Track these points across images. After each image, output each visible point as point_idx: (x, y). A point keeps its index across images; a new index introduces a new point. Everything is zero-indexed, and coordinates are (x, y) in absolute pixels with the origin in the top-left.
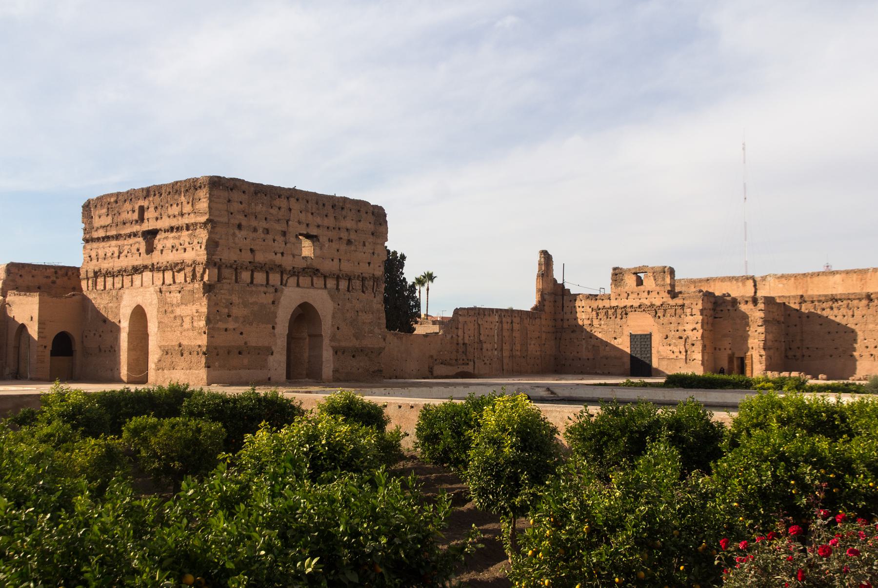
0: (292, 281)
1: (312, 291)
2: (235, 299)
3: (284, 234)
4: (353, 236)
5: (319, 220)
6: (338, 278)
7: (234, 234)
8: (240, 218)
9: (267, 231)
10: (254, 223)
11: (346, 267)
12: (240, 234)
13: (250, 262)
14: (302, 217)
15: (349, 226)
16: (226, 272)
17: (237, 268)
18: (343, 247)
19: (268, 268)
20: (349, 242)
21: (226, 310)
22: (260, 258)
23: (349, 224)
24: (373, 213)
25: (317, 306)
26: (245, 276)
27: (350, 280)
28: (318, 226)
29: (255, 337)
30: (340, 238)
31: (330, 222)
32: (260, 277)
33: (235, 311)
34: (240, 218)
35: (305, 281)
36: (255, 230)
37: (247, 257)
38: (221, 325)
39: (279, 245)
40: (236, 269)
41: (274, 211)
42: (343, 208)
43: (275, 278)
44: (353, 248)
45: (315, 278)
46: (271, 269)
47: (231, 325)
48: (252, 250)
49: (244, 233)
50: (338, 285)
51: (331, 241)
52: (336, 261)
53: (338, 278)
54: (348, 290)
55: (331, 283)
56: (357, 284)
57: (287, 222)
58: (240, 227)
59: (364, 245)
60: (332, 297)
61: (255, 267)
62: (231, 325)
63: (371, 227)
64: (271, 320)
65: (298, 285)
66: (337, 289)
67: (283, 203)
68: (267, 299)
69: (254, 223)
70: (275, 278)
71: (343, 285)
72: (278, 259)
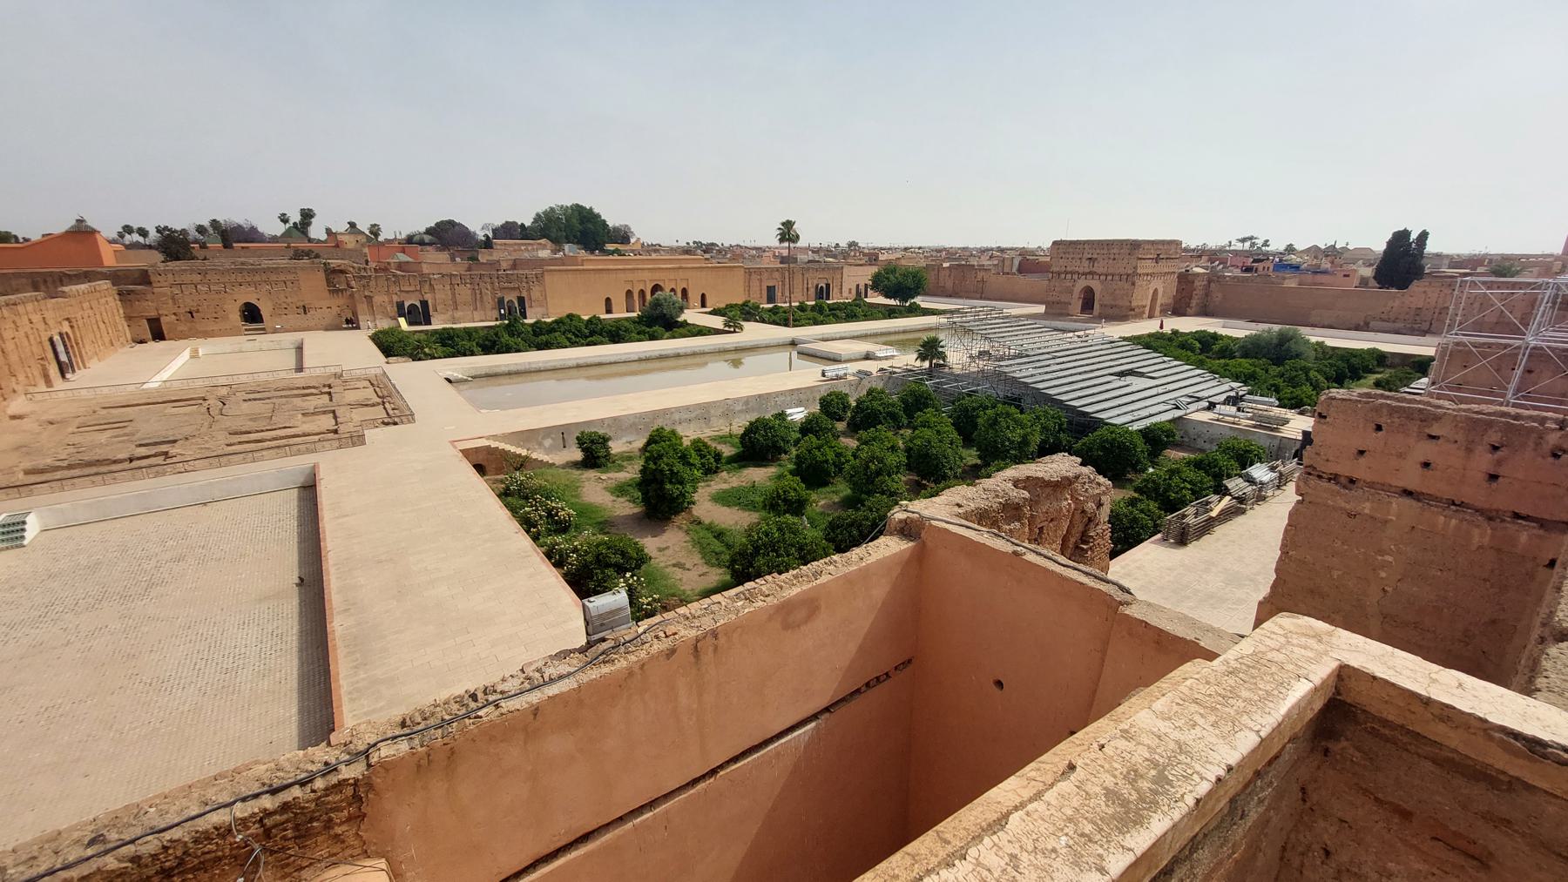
2: (1057, 284)
4: (1117, 256)
5: (1098, 251)
6: (1106, 276)
10: (1067, 256)
17: (1059, 274)
18: (1111, 261)
19: (1072, 273)
20: (1114, 259)
22: (1069, 269)
26: (1063, 276)
29: (1063, 298)
32: (1069, 276)
35: (1089, 277)
43: (1075, 277)
53: (1106, 276)
56: (1117, 278)
60: (1102, 282)
61: (1066, 273)
63: (1129, 251)
64: (1071, 292)
69: (1067, 256)
70: (1075, 277)
71: (1110, 278)
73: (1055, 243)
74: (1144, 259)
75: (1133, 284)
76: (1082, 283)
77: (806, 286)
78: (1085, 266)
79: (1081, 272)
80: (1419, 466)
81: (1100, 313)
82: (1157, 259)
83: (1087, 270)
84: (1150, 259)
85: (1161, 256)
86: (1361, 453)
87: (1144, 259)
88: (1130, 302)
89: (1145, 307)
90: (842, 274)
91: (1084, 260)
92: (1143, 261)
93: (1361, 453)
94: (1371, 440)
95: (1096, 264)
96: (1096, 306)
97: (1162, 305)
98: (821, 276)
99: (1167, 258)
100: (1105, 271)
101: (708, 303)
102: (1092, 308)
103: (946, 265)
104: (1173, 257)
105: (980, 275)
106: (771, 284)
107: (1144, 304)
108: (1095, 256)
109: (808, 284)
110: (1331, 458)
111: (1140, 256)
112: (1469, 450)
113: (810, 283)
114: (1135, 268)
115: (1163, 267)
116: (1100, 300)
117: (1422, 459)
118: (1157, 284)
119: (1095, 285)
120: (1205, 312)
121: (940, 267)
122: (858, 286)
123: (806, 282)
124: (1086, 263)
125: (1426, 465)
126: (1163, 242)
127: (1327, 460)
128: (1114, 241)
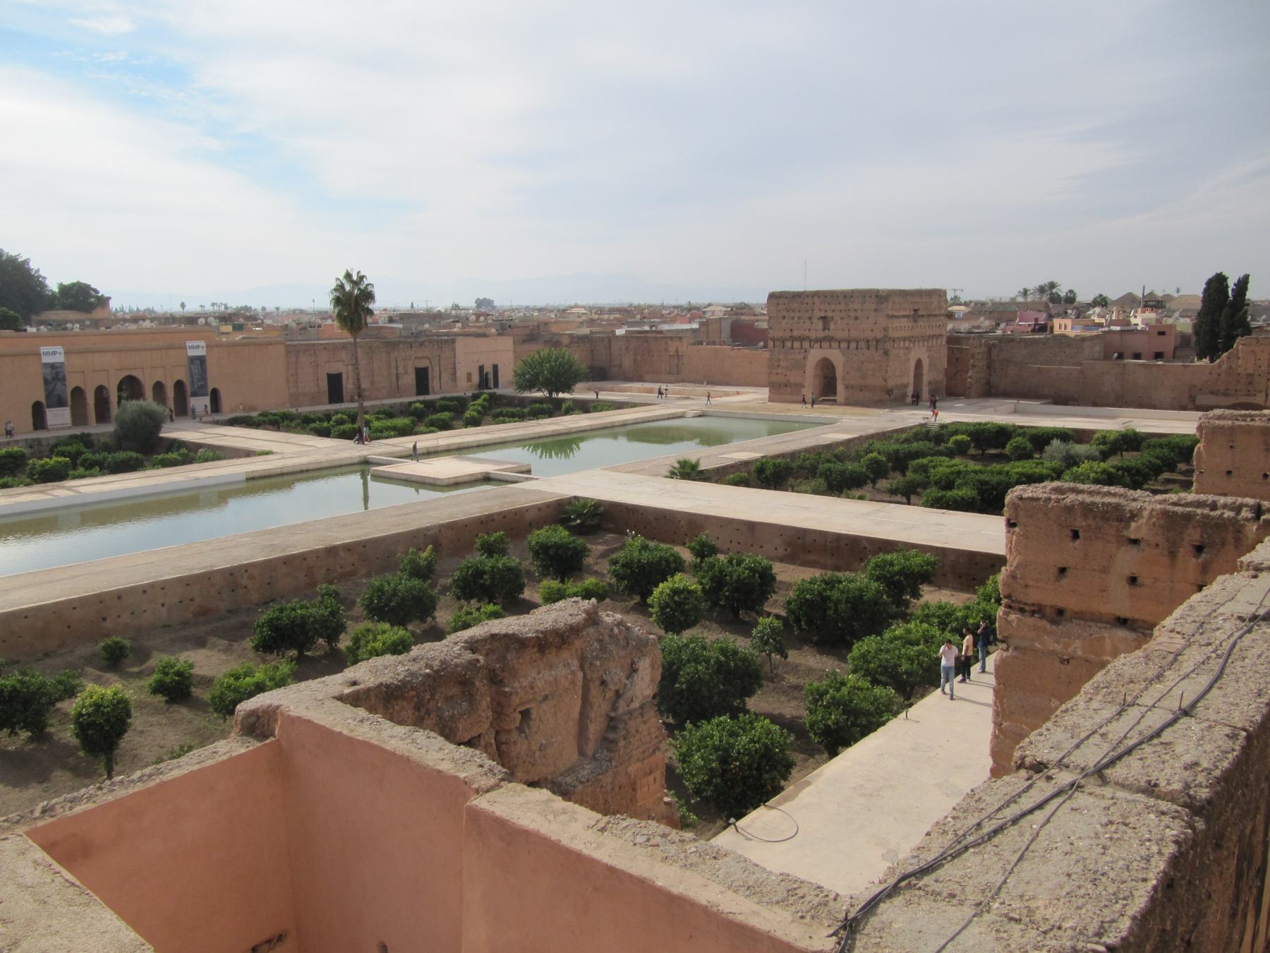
0: (817, 345)
1: (829, 350)
2: (782, 357)
3: (810, 318)
4: (859, 314)
5: (833, 307)
6: (849, 342)
7: (781, 323)
8: (784, 313)
9: (799, 318)
11: (854, 334)
12: (784, 322)
13: (791, 337)
14: (822, 307)
15: (856, 308)
16: (777, 343)
17: (783, 341)
19: (801, 339)
20: (856, 318)
21: (776, 364)
22: (795, 333)
23: (856, 306)
24: (877, 296)
25: (833, 359)
26: (788, 344)
27: (858, 342)
28: (833, 311)
29: (794, 377)
30: (849, 317)
31: (842, 307)
32: (797, 344)
33: (782, 364)
34: (784, 313)
35: (825, 344)
36: (793, 318)
37: (788, 334)
38: (774, 371)
39: (808, 325)
40: (783, 341)
41: (805, 306)
42: (852, 297)
43: (806, 344)
44: (859, 321)
45: (832, 343)
46: (804, 339)
47: (780, 371)
48: (791, 330)
49: (786, 320)
50: (849, 346)
51: (842, 318)
52: (846, 332)
53: (849, 342)
54: (857, 348)
55: (844, 345)
57: (813, 310)
58: (784, 318)
59: (868, 318)
61: (793, 339)
62: (780, 371)
63: (874, 306)
64: (800, 366)
65: (821, 347)
66: (848, 348)
67: (809, 300)
68: (800, 357)
69: (792, 314)
70: (806, 344)
71: (853, 345)
72: (807, 333)
73: (772, 296)
74: (896, 317)
75: (886, 353)
76: (815, 354)
77: (394, 371)
78: (817, 330)
79: (813, 335)
80: (1124, 583)
81: (846, 399)
82: (915, 316)
83: (821, 334)
84: (904, 316)
85: (920, 313)
86: (1063, 571)
87: (899, 317)
88: (885, 380)
89: (906, 386)
90: (454, 350)
91: (815, 320)
92: (896, 320)
93: (1063, 571)
94: (1070, 552)
95: (832, 326)
96: (840, 388)
97: (930, 383)
98: (420, 355)
99: (929, 316)
100: (844, 335)
101: (226, 401)
102: (834, 392)
103: (620, 332)
104: (937, 312)
105: (673, 346)
106: (334, 371)
107: (906, 382)
108: (829, 314)
109: (397, 368)
110: (1031, 583)
111: (890, 313)
112: (1173, 555)
113: (401, 365)
114: (886, 329)
115: (924, 328)
116: (844, 379)
117: (1127, 573)
118: (918, 352)
119: (836, 356)
120: (990, 391)
121: (612, 338)
122: (481, 368)
123: (393, 365)
124: (820, 325)
125: (1133, 580)
126: (919, 293)
127: (1026, 586)
128: (853, 291)
